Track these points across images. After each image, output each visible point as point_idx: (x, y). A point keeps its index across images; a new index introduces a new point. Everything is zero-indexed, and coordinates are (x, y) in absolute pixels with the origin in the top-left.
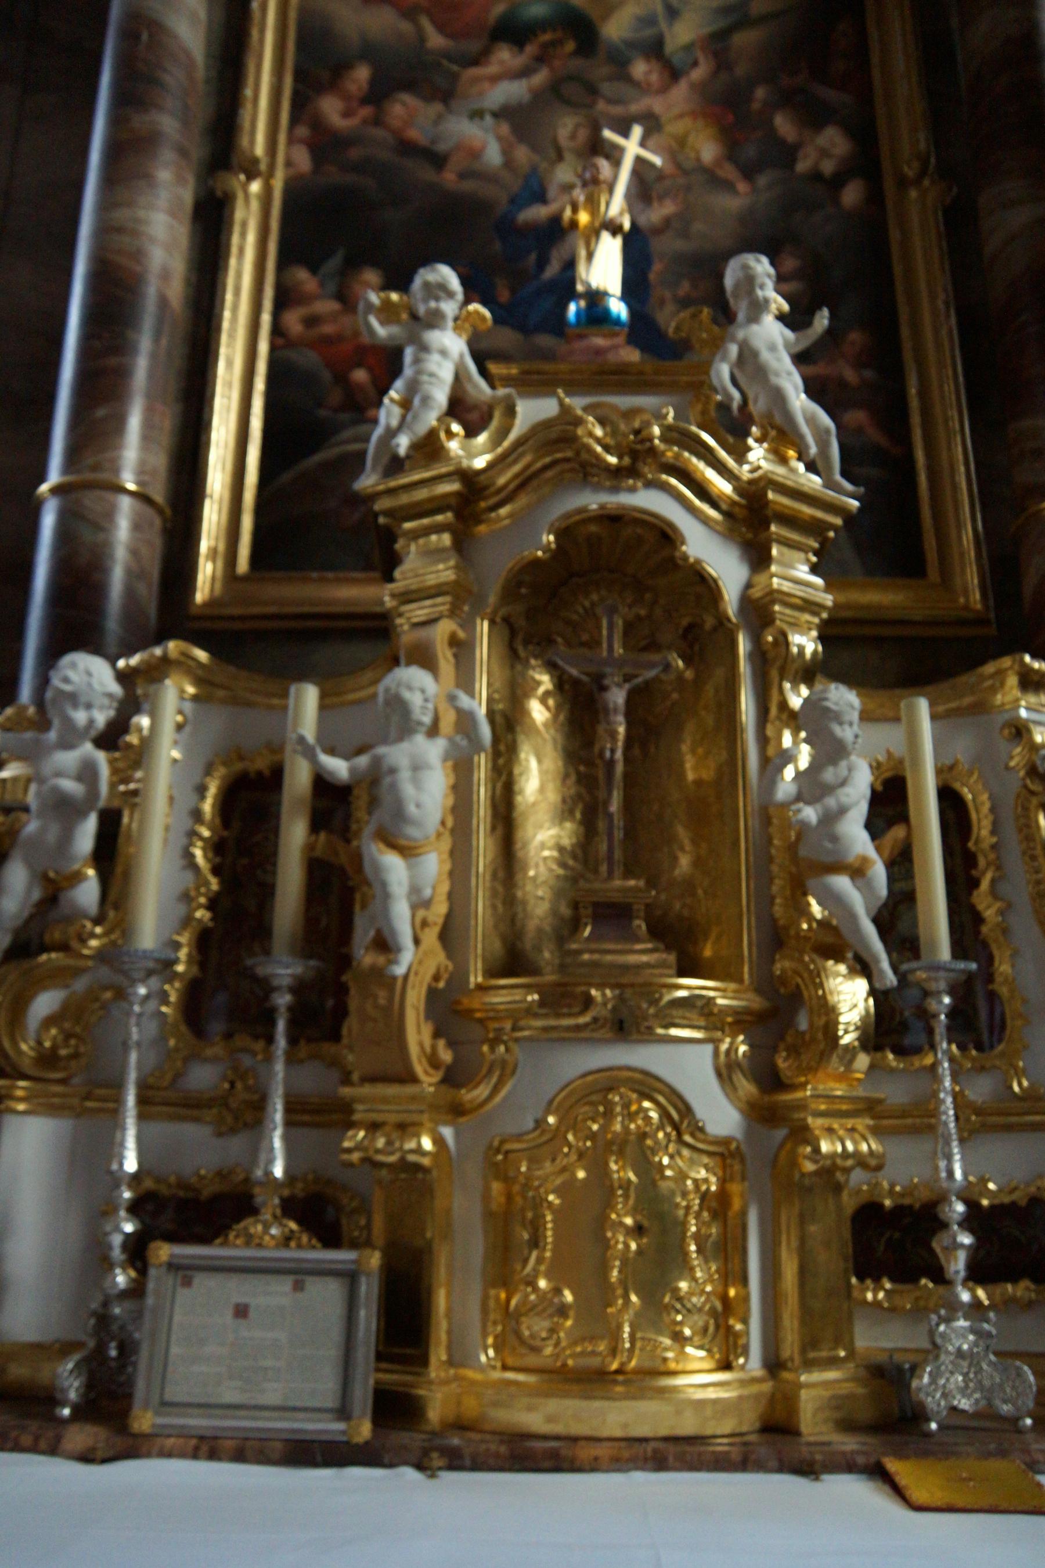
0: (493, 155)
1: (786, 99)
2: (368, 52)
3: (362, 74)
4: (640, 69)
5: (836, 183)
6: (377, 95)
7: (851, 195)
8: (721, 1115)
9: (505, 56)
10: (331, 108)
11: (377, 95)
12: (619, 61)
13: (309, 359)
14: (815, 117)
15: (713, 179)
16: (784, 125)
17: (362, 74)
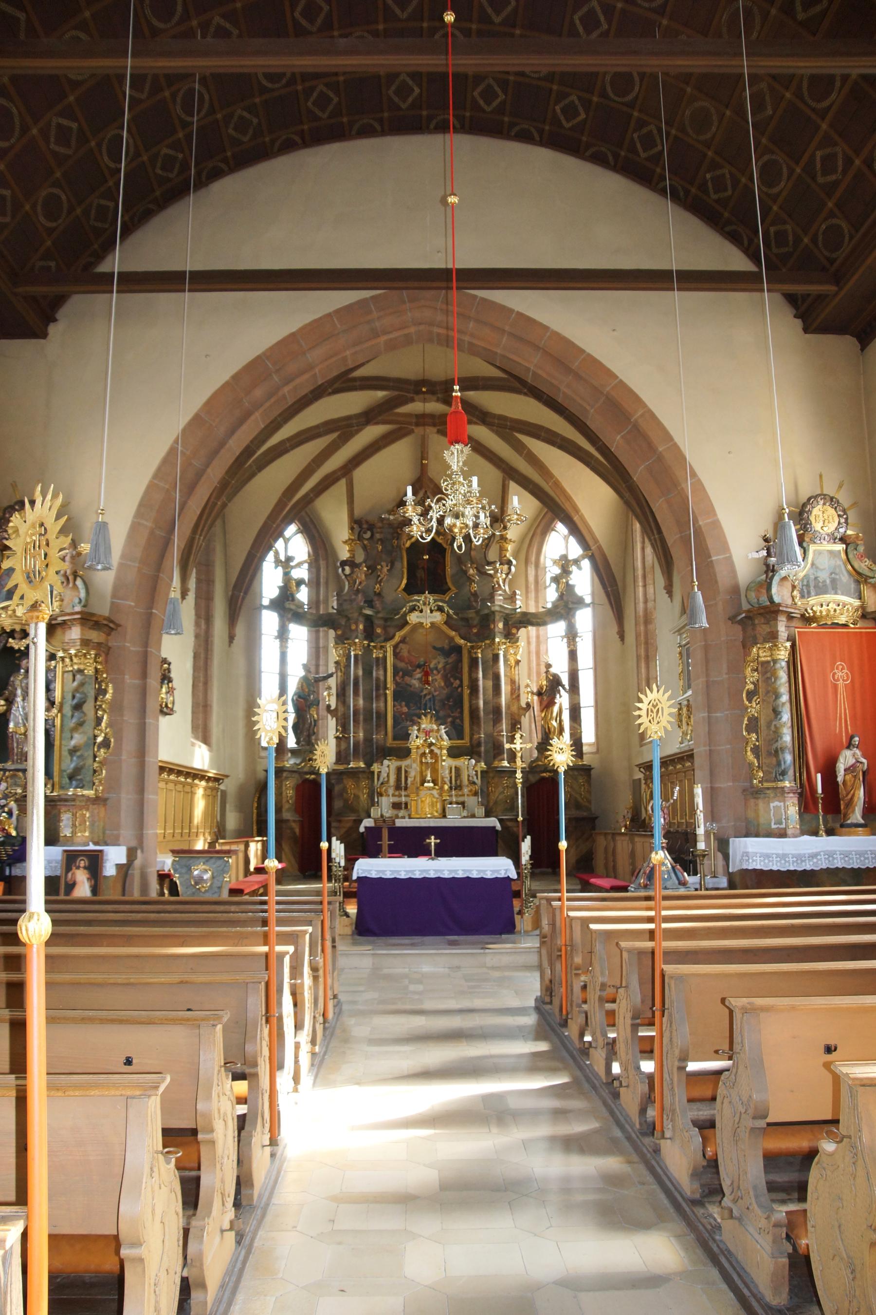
0: (417, 685)
1: (452, 676)
2: (402, 670)
3: (401, 673)
4: (435, 672)
5: (457, 688)
6: (403, 677)
7: (459, 690)
8: (437, 796)
9: (418, 670)
10: (397, 678)
11: (403, 677)
12: (432, 670)
13: (397, 714)
14: (455, 679)
15: (442, 687)
16: (452, 680)
17: (401, 673)
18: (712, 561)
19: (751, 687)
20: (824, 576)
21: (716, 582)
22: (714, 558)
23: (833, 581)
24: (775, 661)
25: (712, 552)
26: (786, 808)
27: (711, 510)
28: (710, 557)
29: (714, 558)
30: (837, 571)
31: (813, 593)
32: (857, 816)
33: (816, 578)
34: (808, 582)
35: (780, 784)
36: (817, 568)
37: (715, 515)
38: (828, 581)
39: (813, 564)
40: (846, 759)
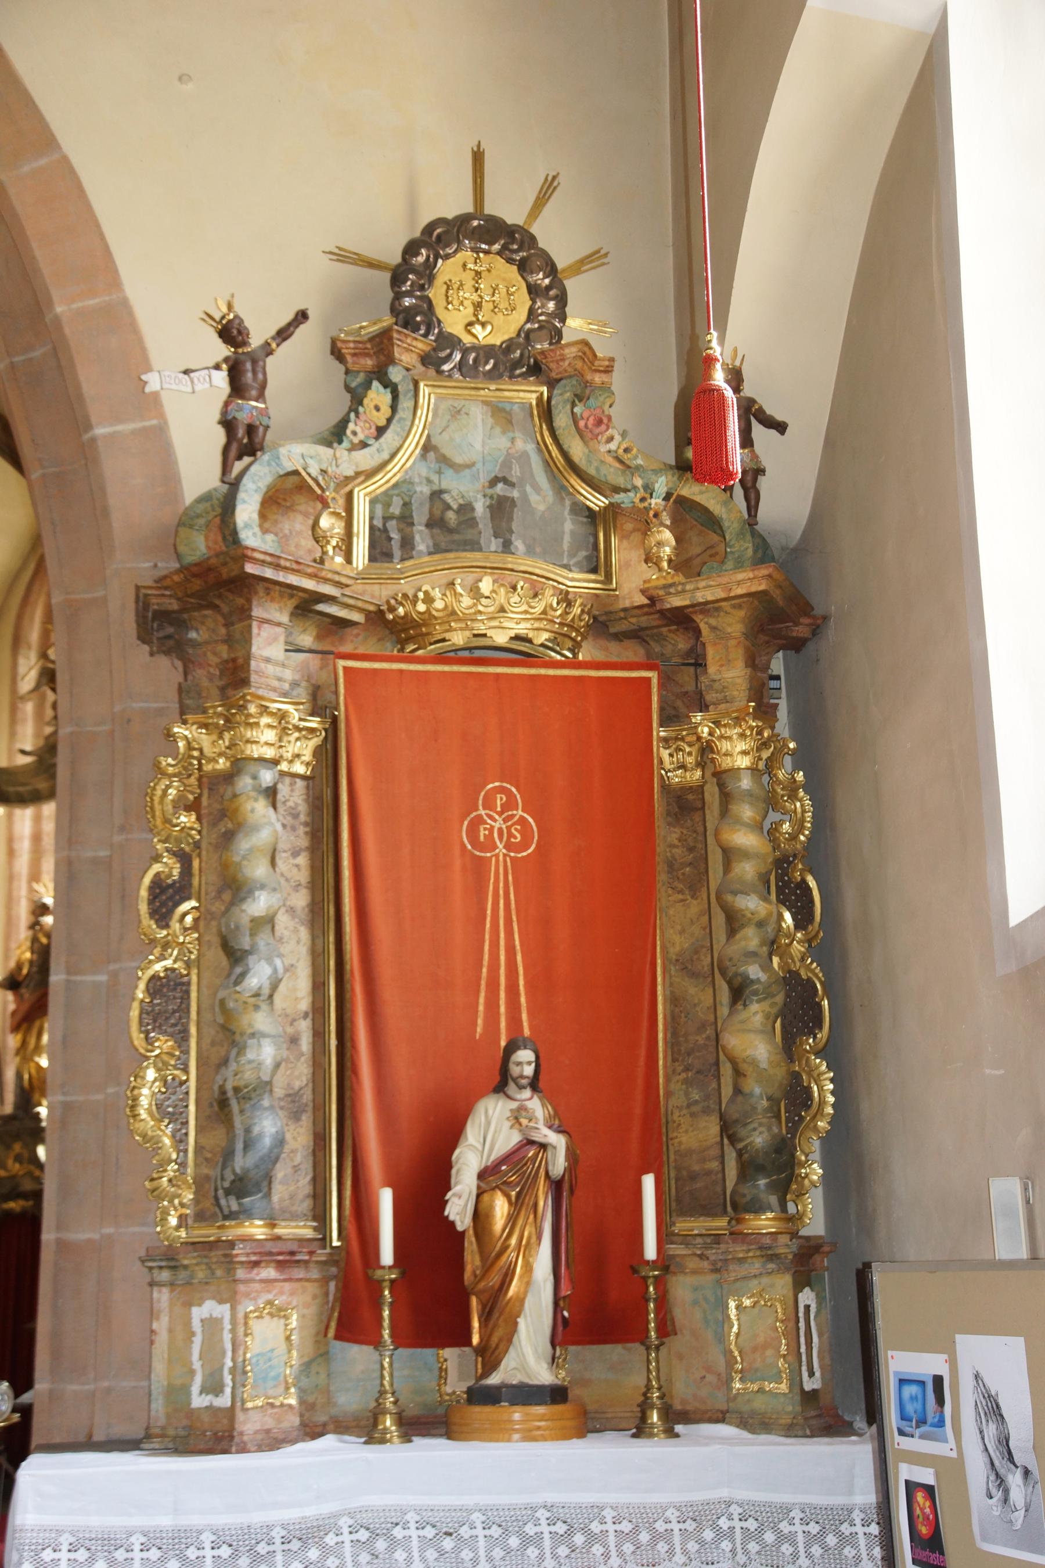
18: (93, 440)
19: (168, 867)
20: (465, 488)
21: (106, 513)
22: (100, 431)
23: (501, 509)
24: (239, 765)
25: (95, 410)
26: (241, 1327)
27: (102, 268)
28: (89, 427)
29: (100, 431)
30: (515, 473)
31: (422, 541)
32: (529, 1354)
33: (436, 495)
34: (406, 505)
35: (233, 1231)
36: (444, 460)
37: (114, 281)
38: (480, 507)
39: (428, 448)
40: (490, 1131)
